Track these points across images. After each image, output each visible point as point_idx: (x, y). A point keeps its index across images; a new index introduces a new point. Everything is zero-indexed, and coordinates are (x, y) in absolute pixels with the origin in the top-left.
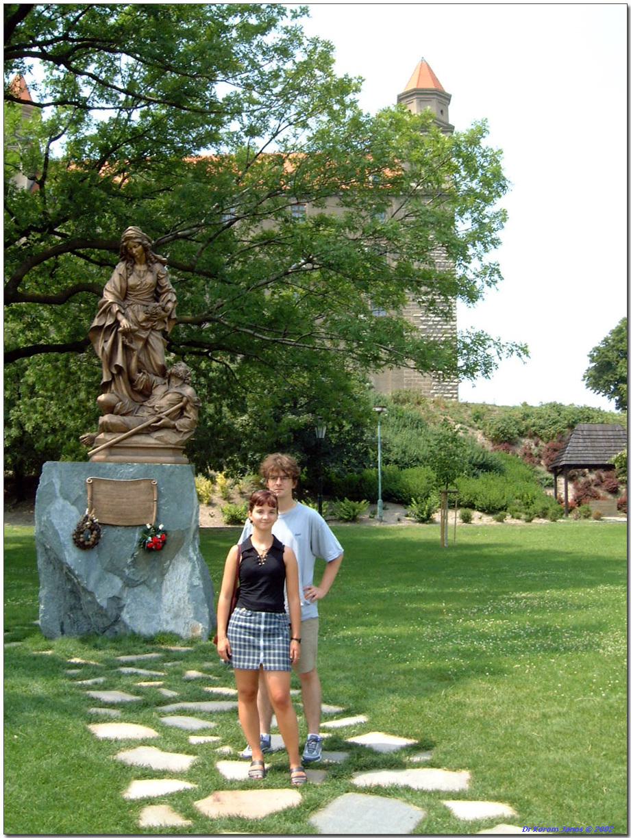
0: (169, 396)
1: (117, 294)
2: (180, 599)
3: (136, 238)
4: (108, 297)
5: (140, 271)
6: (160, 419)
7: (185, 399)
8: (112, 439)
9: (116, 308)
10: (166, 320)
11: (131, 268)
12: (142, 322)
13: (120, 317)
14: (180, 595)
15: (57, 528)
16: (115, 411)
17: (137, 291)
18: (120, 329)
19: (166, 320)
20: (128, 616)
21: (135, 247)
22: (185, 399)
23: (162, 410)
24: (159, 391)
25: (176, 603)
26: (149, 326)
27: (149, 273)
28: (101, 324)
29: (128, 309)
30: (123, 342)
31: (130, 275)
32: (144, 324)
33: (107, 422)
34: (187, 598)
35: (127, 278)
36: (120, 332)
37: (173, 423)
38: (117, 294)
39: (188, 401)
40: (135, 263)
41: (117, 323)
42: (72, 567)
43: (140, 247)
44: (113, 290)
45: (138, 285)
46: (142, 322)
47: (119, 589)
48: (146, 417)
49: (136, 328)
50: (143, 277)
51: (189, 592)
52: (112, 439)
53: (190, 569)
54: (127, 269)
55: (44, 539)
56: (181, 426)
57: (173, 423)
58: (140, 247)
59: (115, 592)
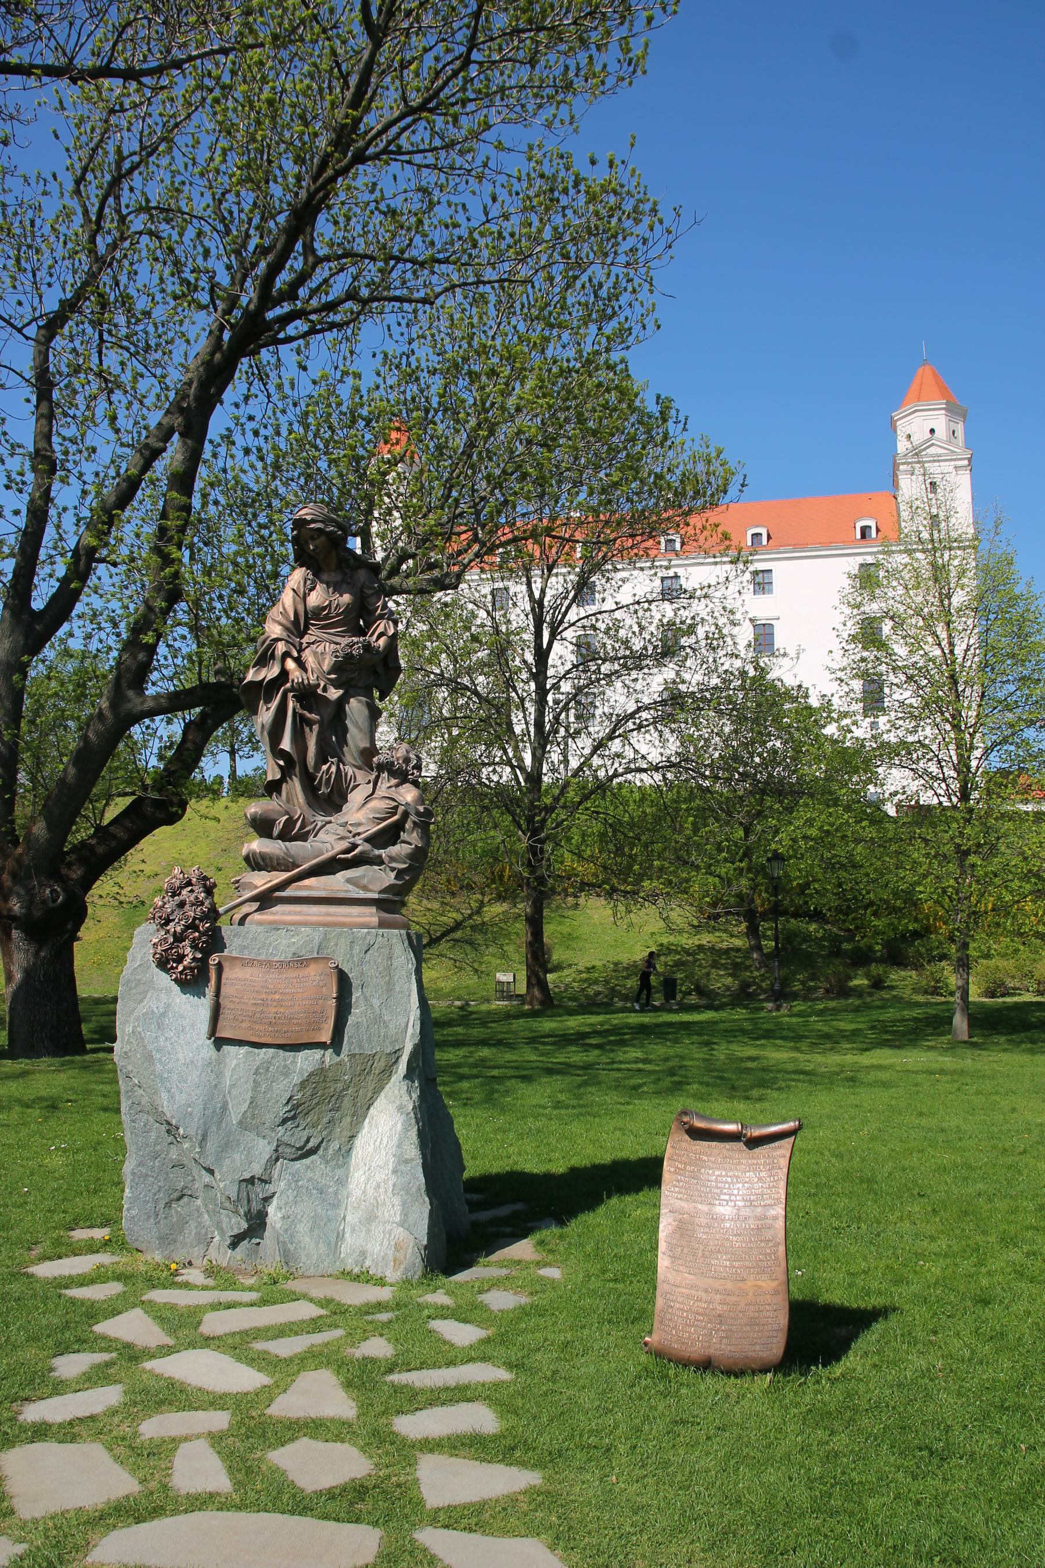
0: (374, 804)
1: (289, 625)
2: (378, 1186)
3: (313, 521)
4: (274, 630)
6: (354, 846)
7: (401, 809)
8: (262, 881)
9: (281, 647)
10: (380, 669)
13: (290, 664)
14: (380, 1177)
15: (150, 1047)
16: (276, 832)
17: (327, 617)
19: (380, 669)
20: (280, 1215)
21: (313, 538)
22: (401, 809)
23: (360, 830)
24: (356, 797)
25: (370, 1192)
28: (260, 678)
29: (307, 651)
30: (294, 709)
33: (254, 853)
34: (391, 1183)
37: (377, 852)
38: (289, 625)
39: (406, 815)
41: (284, 673)
42: (174, 1122)
43: (323, 538)
44: (280, 618)
47: (263, 1161)
48: (328, 840)
51: (394, 1172)
52: (262, 881)
53: (399, 1126)
55: (130, 1068)
56: (392, 859)
57: (377, 852)
59: (257, 1169)
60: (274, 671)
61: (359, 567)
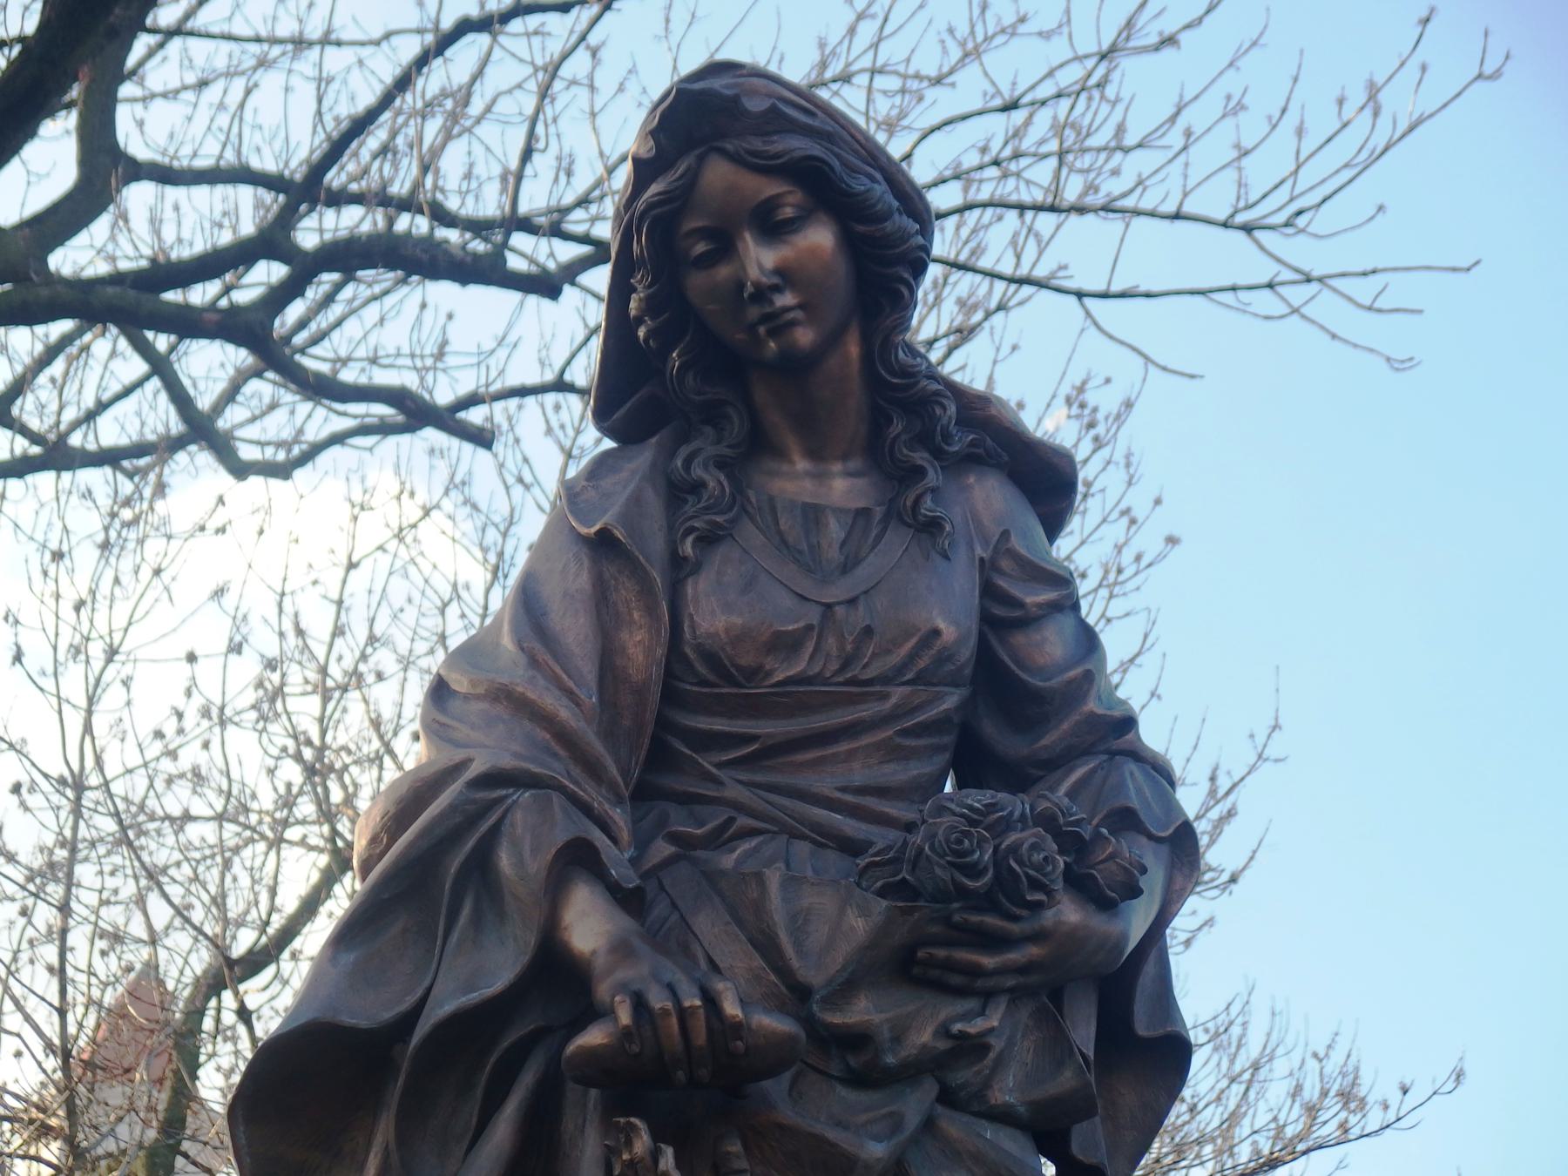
5: (813, 515)
11: (715, 481)
12: (845, 989)
18: (594, 1037)
26: (924, 1037)
27: (896, 542)
31: (709, 540)
32: (862, 1011)
35: (679, 569)
36: (597, 1069)
40: (758, 445)
45: (785, 644)
46: (845, 989)
49: (772, 1023)
50: (846, 568)
54: (678, 492)
58: (820, 238)
60: (486, 968)
61: (974, 460)
